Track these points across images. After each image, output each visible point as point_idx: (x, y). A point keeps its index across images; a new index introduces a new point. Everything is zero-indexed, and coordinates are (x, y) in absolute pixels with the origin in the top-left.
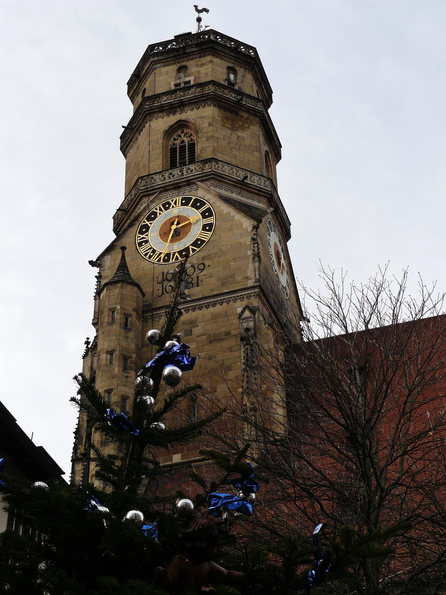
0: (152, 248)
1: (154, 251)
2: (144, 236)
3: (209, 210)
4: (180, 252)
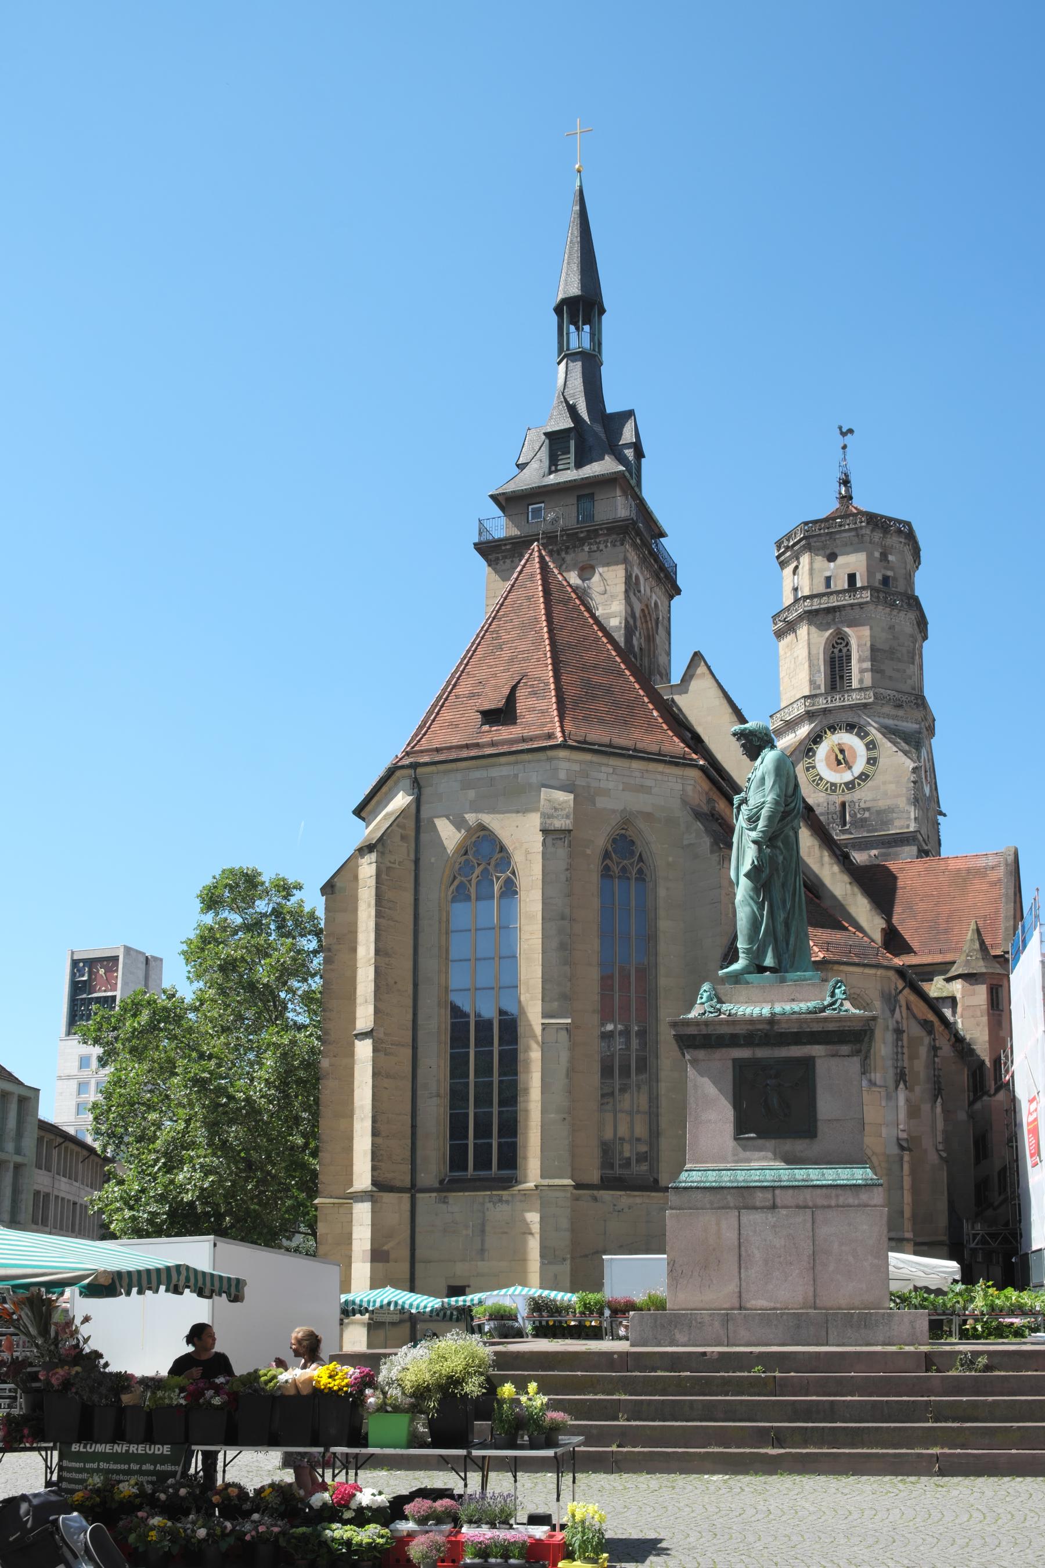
0: (818, 775)
1: (821, 779)
2: (810, 761)
3: (872, 742)
4: (846, 784)
